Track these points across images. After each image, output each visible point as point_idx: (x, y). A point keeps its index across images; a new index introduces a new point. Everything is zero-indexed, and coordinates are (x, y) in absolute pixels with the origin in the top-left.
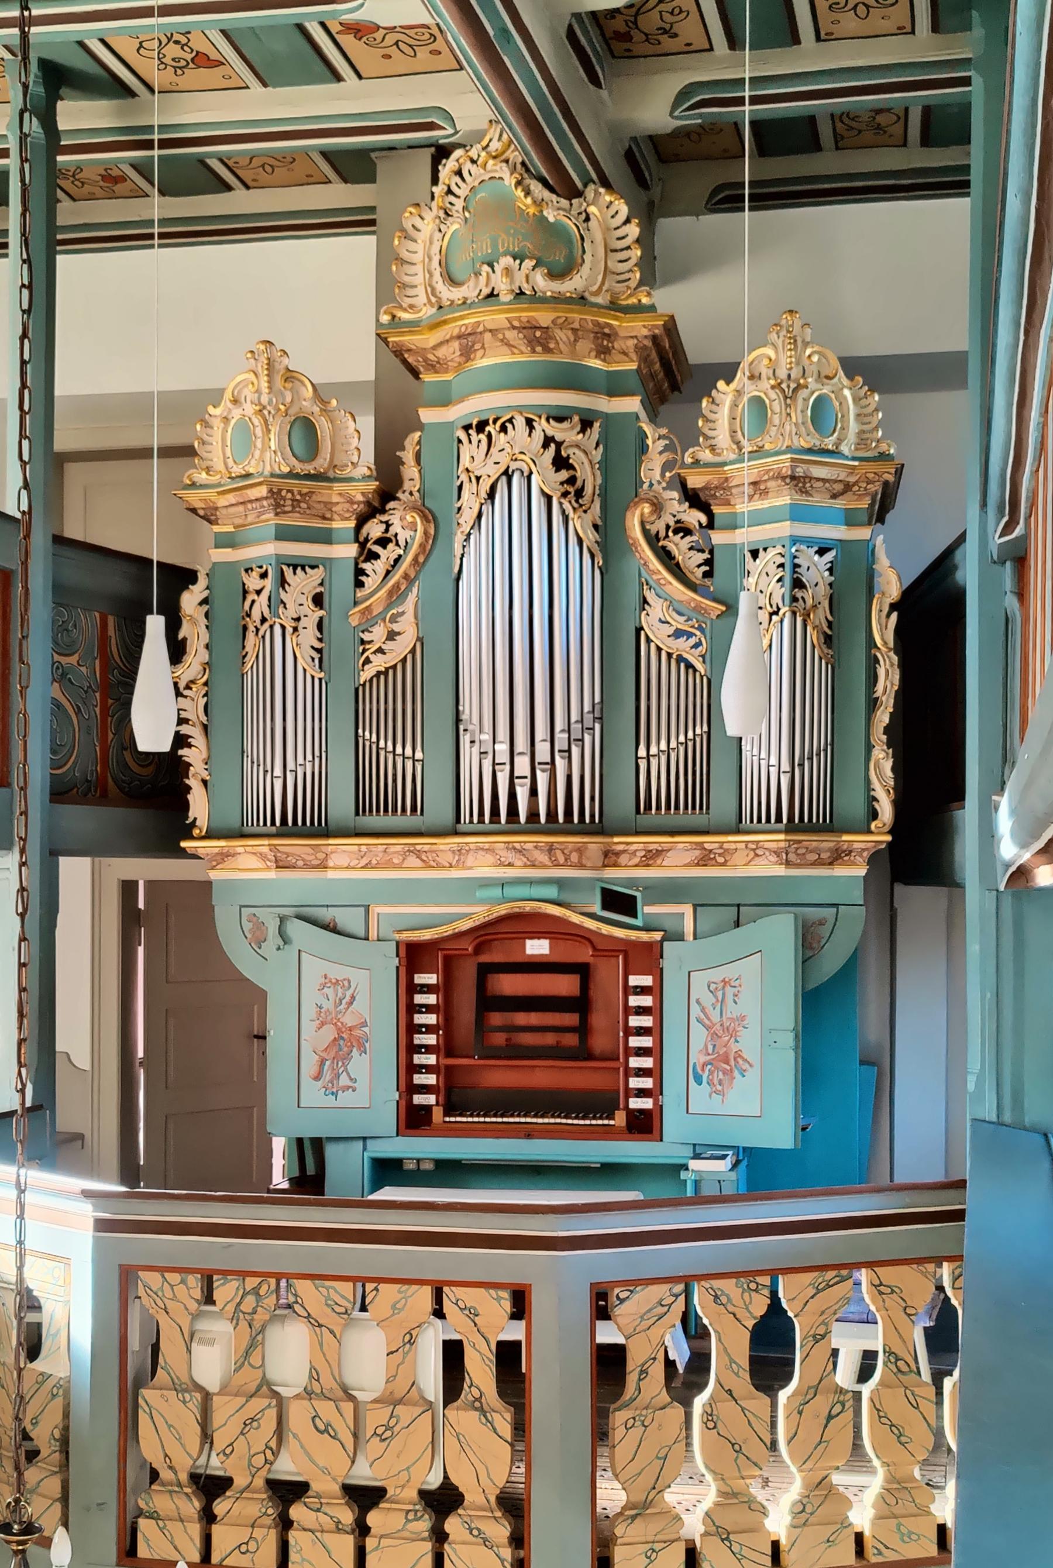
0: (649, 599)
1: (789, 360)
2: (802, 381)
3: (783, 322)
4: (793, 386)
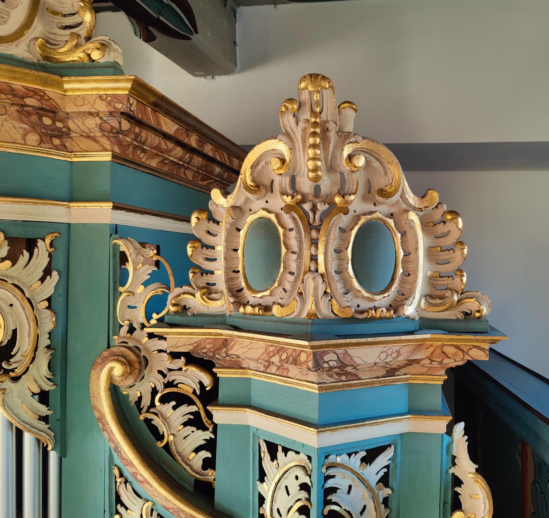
0: (124, 499)
1: (311, 164)
2: (338, 200)
3: (305, 96)
4: (322, 207)
